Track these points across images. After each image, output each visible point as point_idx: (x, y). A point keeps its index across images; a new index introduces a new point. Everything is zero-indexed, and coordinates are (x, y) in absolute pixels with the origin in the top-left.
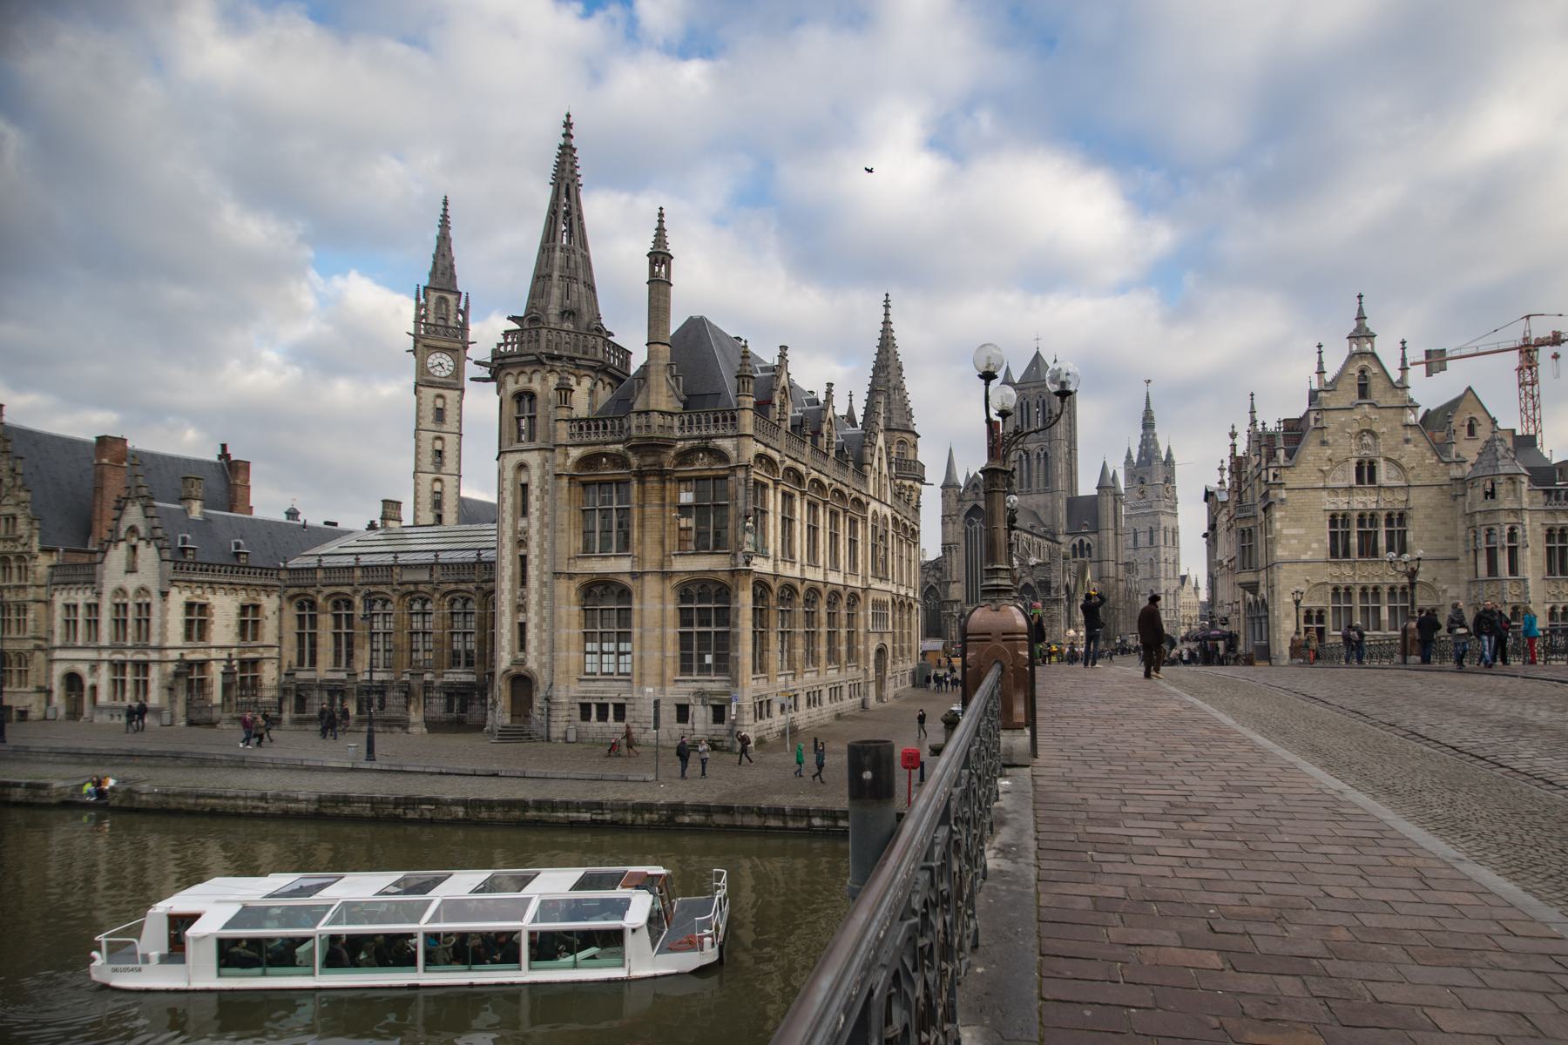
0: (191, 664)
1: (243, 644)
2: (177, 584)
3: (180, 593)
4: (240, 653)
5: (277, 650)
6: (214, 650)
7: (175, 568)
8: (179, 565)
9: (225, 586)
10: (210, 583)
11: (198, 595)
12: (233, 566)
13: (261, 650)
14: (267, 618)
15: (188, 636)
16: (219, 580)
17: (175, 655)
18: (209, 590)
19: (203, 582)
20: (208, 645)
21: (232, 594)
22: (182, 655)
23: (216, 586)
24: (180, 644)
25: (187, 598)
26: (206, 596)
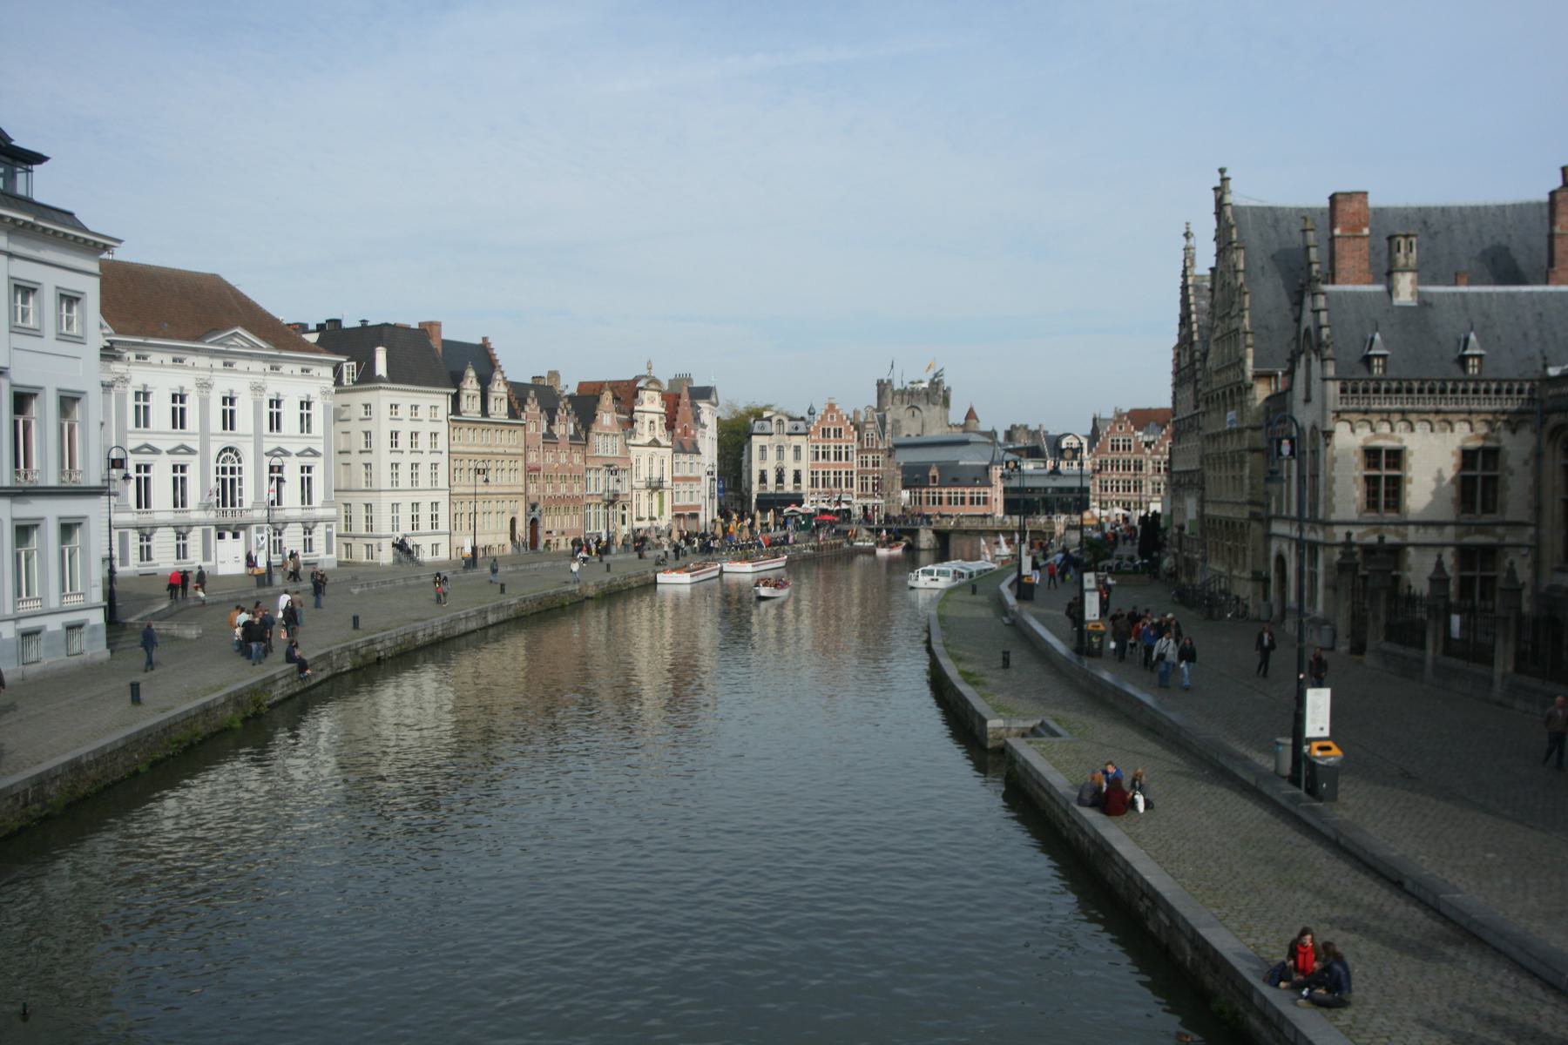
0: (1368, 550)
1: (1465, 518)
2: (1346, 416)
3: (1353, 430)
4: (1458, 536)
5: (1531, 530)
6: (1412, 529)
7: (1343, 391)
8: (1350, 385)
9: (1431, 417)
10: (1403, 412)
11: (1386, 436)
12: (1456, 381)
13: (1500, 530)
14: (1511, 473)
15: (1372, 503)
16: (1420, 406)
17: (1339, 534)
18: (1403, 425)
19: (1389, 412)
20: (1403, 519)
21: (1444, 430)
22: (1349, 535)
23: (1413, 417)
24: (1354, 516)
25: (1365, 440)
26: (1397, 434)
